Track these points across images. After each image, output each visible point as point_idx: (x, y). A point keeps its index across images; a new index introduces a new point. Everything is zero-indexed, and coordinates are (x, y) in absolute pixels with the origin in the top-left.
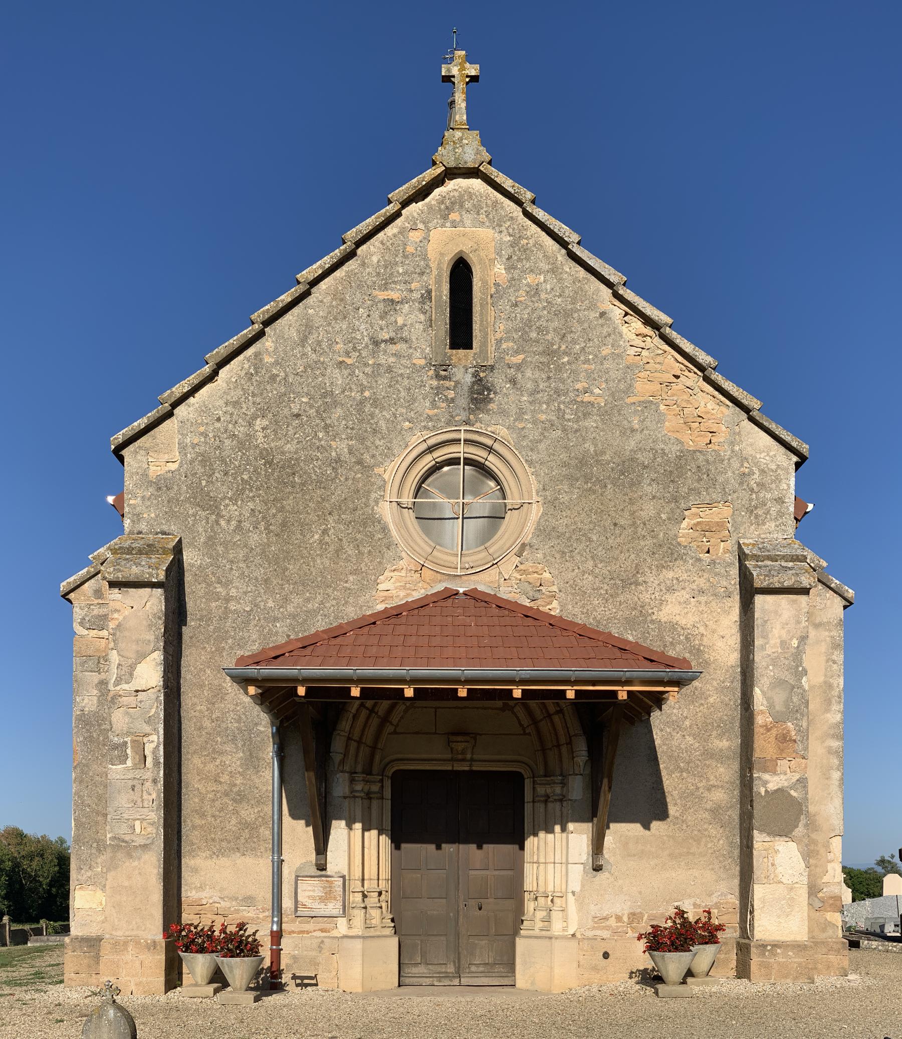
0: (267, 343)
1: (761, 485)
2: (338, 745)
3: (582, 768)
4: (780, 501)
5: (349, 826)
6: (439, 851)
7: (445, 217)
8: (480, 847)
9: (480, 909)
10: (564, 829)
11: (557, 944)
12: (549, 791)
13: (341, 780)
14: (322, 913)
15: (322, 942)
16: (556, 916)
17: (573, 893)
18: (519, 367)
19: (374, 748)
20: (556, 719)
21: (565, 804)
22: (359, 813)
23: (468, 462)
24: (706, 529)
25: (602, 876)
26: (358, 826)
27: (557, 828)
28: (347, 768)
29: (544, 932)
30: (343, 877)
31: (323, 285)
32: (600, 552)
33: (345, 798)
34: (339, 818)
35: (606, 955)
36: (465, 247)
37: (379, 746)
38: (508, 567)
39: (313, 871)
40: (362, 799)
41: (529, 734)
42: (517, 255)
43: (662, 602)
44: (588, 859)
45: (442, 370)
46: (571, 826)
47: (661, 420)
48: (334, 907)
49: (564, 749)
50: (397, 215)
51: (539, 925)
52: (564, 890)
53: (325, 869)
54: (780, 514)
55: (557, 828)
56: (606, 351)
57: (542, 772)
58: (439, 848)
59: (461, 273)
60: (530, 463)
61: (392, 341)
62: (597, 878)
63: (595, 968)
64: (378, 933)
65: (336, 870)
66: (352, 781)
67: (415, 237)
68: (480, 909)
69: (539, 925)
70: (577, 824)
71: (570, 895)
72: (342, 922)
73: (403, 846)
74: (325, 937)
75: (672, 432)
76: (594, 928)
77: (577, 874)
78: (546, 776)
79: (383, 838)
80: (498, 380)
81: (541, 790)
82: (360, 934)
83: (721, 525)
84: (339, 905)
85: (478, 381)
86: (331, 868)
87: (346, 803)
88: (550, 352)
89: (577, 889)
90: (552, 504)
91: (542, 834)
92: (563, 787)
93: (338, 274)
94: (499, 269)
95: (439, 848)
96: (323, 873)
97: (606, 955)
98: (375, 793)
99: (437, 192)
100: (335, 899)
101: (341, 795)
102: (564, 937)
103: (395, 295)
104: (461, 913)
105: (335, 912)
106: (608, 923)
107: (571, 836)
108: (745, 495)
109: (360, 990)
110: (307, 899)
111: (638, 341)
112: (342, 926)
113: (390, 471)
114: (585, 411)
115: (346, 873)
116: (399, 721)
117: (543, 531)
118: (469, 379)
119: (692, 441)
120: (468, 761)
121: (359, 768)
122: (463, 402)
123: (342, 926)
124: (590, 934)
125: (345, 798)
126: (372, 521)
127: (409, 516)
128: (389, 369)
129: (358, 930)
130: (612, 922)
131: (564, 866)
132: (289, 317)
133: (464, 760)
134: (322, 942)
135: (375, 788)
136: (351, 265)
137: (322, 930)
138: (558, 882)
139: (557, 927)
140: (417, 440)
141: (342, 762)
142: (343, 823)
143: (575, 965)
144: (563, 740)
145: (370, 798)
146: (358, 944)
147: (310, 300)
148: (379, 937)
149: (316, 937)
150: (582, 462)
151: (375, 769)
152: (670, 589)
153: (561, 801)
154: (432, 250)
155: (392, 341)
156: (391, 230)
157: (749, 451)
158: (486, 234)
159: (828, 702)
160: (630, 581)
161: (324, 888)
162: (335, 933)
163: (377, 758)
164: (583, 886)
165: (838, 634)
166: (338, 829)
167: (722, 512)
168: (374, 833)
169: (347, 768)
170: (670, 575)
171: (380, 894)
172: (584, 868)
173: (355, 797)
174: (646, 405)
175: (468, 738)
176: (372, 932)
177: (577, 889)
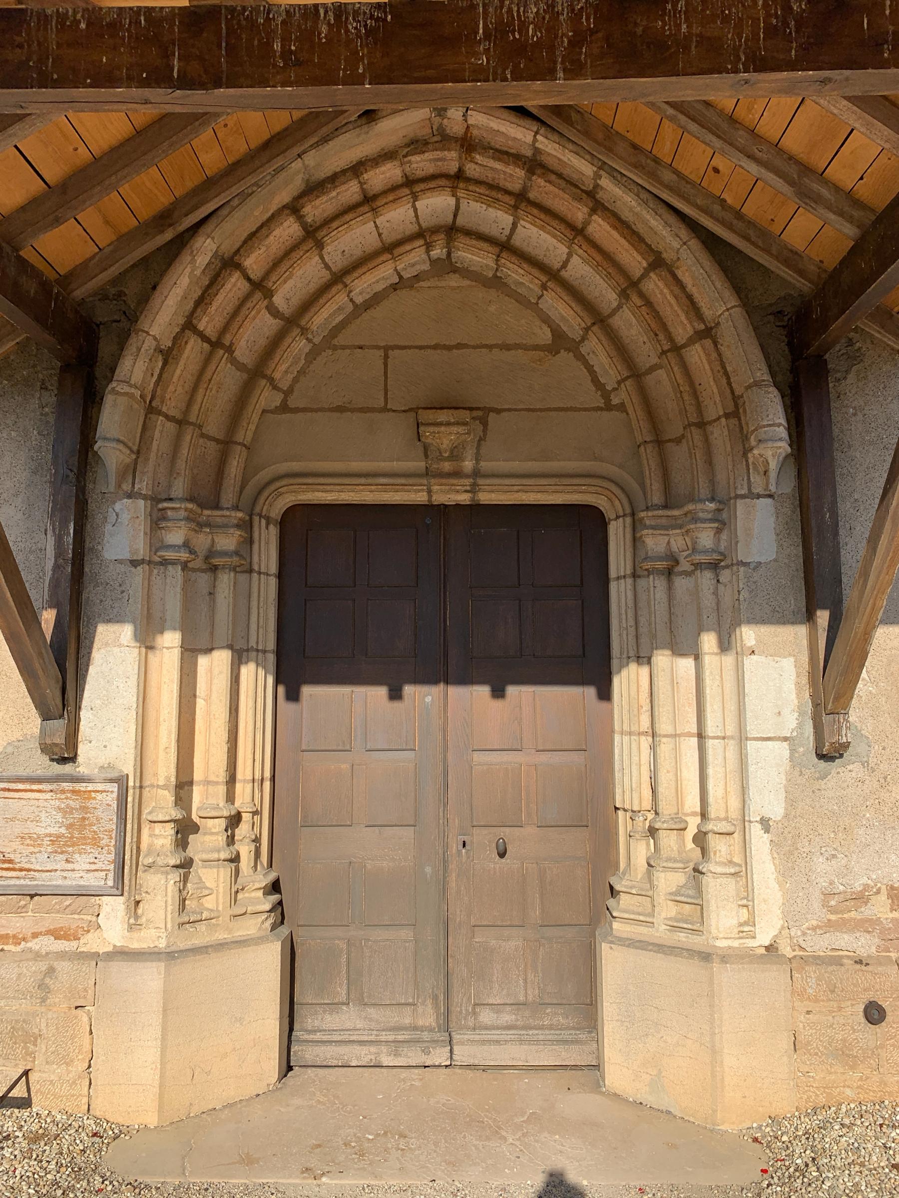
2: (114, 419)
3: (773, 475)
5: (146, 642)
6: (396, 704)
8: (498, 693)
9: (502, 855)
10: (724, 646)
11: (728, 978)
12: (678, 542)
13: (125, 517)
14: (56, 880)
15: (51, 971)
16: (719, 889)
17: (765, 823)
19: (226, 444)
20: (697, 355)
21: (725, 575)
22: (173, 604)
25: (845, 772)
26: (171, 640)
27: (709, 641)
28: (143, 485)
29: (682, 936)
30: (121, 781)
33: (134, 563)
34: (118, 619)
35: (874, 1014)
37: (239, 437)
39: (42, 765)
40: (185, 566)
41: (622, 407)
44: (800, 726)
46: (748, 635)
48: (90, 867)
49: (719, 434)
51: (667, 910)
52: (734, 813)
53: (73, 759)
55: (709, 641)
57: (657, 498)
58: (395, 695)
62: (831, 782)
63: (845, 1055)
64: (221, 936)
65: (102, 761)
66: (157, 522)
68: (502, 855)
69: (667, 910)
70: (766, 631)
71: (756, 830)
72: (113, 909)
73: (307, 691)
74: (62, 955)
76: (829, 926)
77: (772, 770)
78: (666, 507)
79: (214, 666)
81: (655, 543)
82: (162, 944)
84: (106, 860)
86: (90, 755)
87: (138, 575)
89: (776, 810)
91: (662, 659)
92: (719, 531)
95: (395, 695)
96: (68, 768)
97: (874, 1014)
98: (225, 554)
100: (95, 842)
101: (127, 556)
102: (745, 957)
104: (452, 866)
105: (93, 881)
106: (867, 911)
107: (750, 662)
109: (152, 1120)
110: (16, 845)
112: (112, 925)
115: (128, 768)
116: (296, 380)
120: (467, 476)
121: (179, 488)
123: (112, 925)
124: (820, 944)
125: (134, 563)
129: (155, 934)
130: (880, 908)
131: (732, 745)
133: (457, 474)
134: (51, 971)
135: (228, 541)
137: (57, 934)
138: (715, 790)
139: (723, 924)
141: (131, 470)
142: (126, 632)
143: (785, 1043)
144: (714, 408)
145: (214, 569)
146: (150, 979)
148: (221, 946)
149: (37, 956)
151: (228, 497)
153: (715, 566)
161: (66, 811)
162: (92, 943)
163: (234, 468)
164: (791, 802)
166: (113, 652)
168: (221, 658)
169: (143, 485)
171: (235, 820)
172: (793, 751)
173: (165, 563)
175: (466, 415)
176: (202, 936)
177: (776, 810)
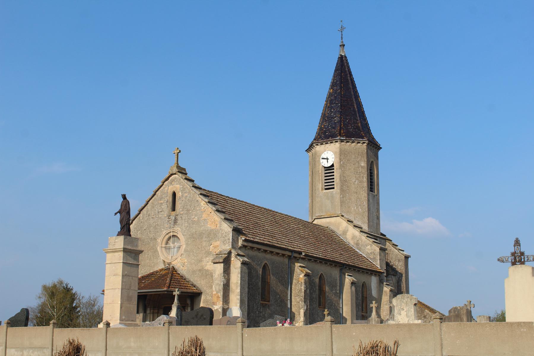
0: (141, 215)
1: (225, 236)
4: (229, 239)
7: (171, 184)
18: (182, 214)
23: (173, 236)
24: (215, 247)
31: (150, 201)
32: (195, 255)
36: (174, 189)
38: (179, 260)
42: (183, 190)
43: (206, 265)
45: (169, 216)
47: (207, 223)
50: (163, 185)
54: (229, 242)
56: (198, 209)
59: (174, 194)
60: (184, 235)
61: (161, 212)
67: (166, 188)
75: (210, 226)
80: (179, 218)
83: (218, 246)
85: (175, 218)
88: (188, 210)
90: (187, 244)
93: (153, 199)
94: (180, 193)
99: (170, 178)
103: (162, 202)
108: (222, 239)
111: (204, 206)
113: (159, 240)
114: (194, 222)
117: (186, 251)
118: (174, 218)
119: (213, 227)
122: (172, 223)
126: (156, 251)
127: (163, 249)
128: (160, 218)
132: (145, 209)
135: (157, 311)
136: (155, 196)
140: (165, 232)
147: (148, 205)
150: (193, 234)
152: (208, 262)
154: (169, 192)
155: (161, 212)
156: (162, 188)
157: (223, 228)
158: (178, 186)
159: (237, 287)
160: (200, 261)
165: (239, 270)
167: (218, 243)
170: (208, 258)
174: (205, 220)
